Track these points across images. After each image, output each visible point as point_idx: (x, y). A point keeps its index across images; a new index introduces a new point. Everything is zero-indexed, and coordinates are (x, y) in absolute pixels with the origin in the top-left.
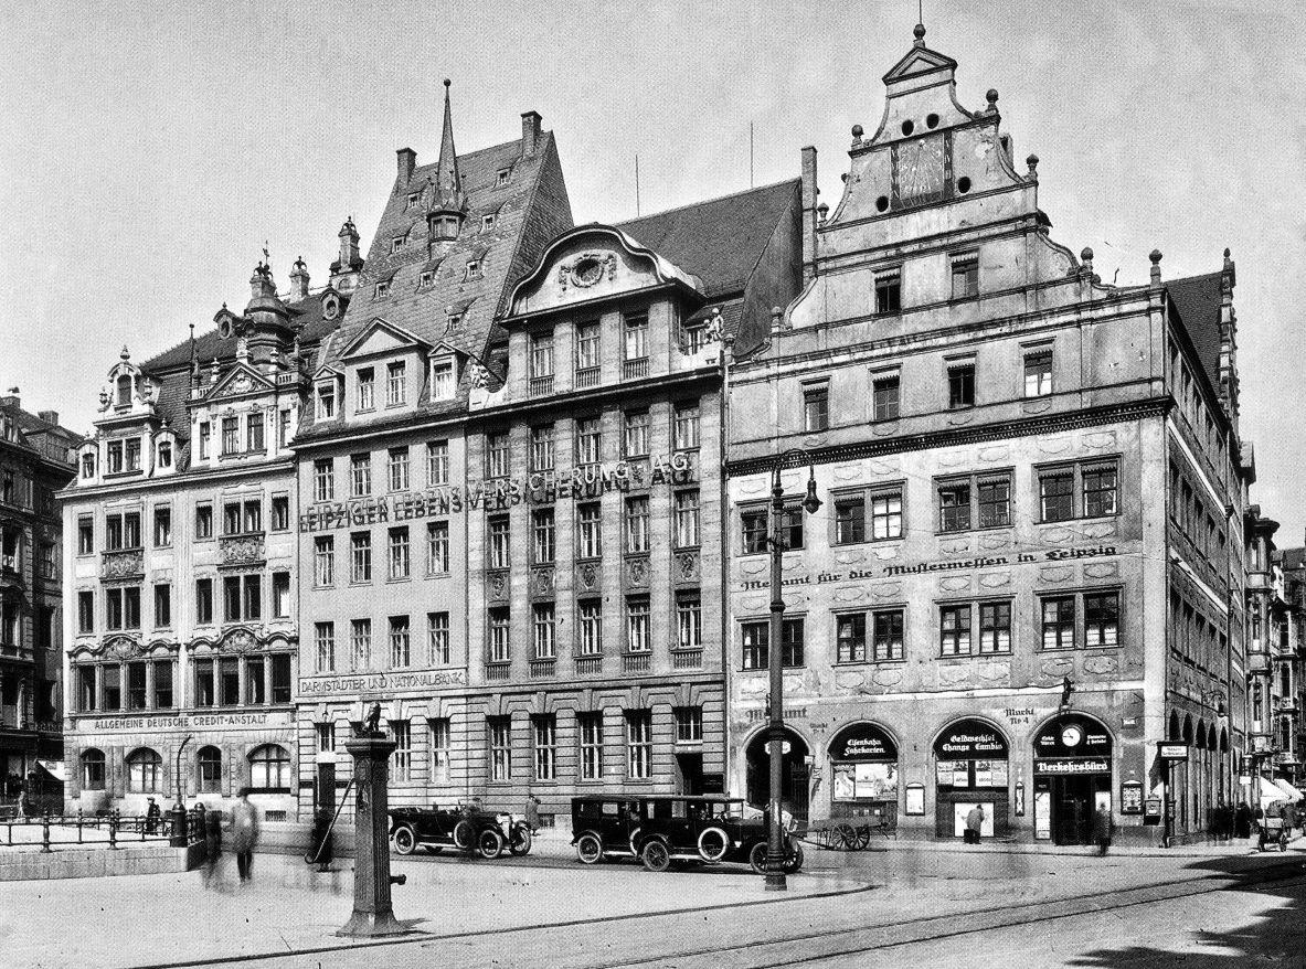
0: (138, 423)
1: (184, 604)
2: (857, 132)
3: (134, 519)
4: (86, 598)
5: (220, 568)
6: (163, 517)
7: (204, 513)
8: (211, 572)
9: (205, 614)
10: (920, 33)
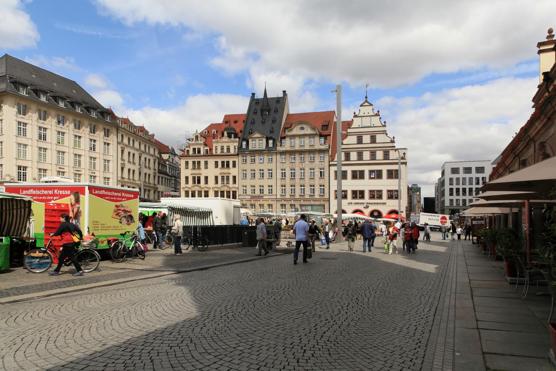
0: (200, 144)
1: (211, 181)
2: (355, 113)
3: (199, 163)
4: (187, 178)
5: (220, 174)
6: (206, 163)
7: (216, 163)
8: (217, 174)
9: (217, 182)
10: (366, 98)
